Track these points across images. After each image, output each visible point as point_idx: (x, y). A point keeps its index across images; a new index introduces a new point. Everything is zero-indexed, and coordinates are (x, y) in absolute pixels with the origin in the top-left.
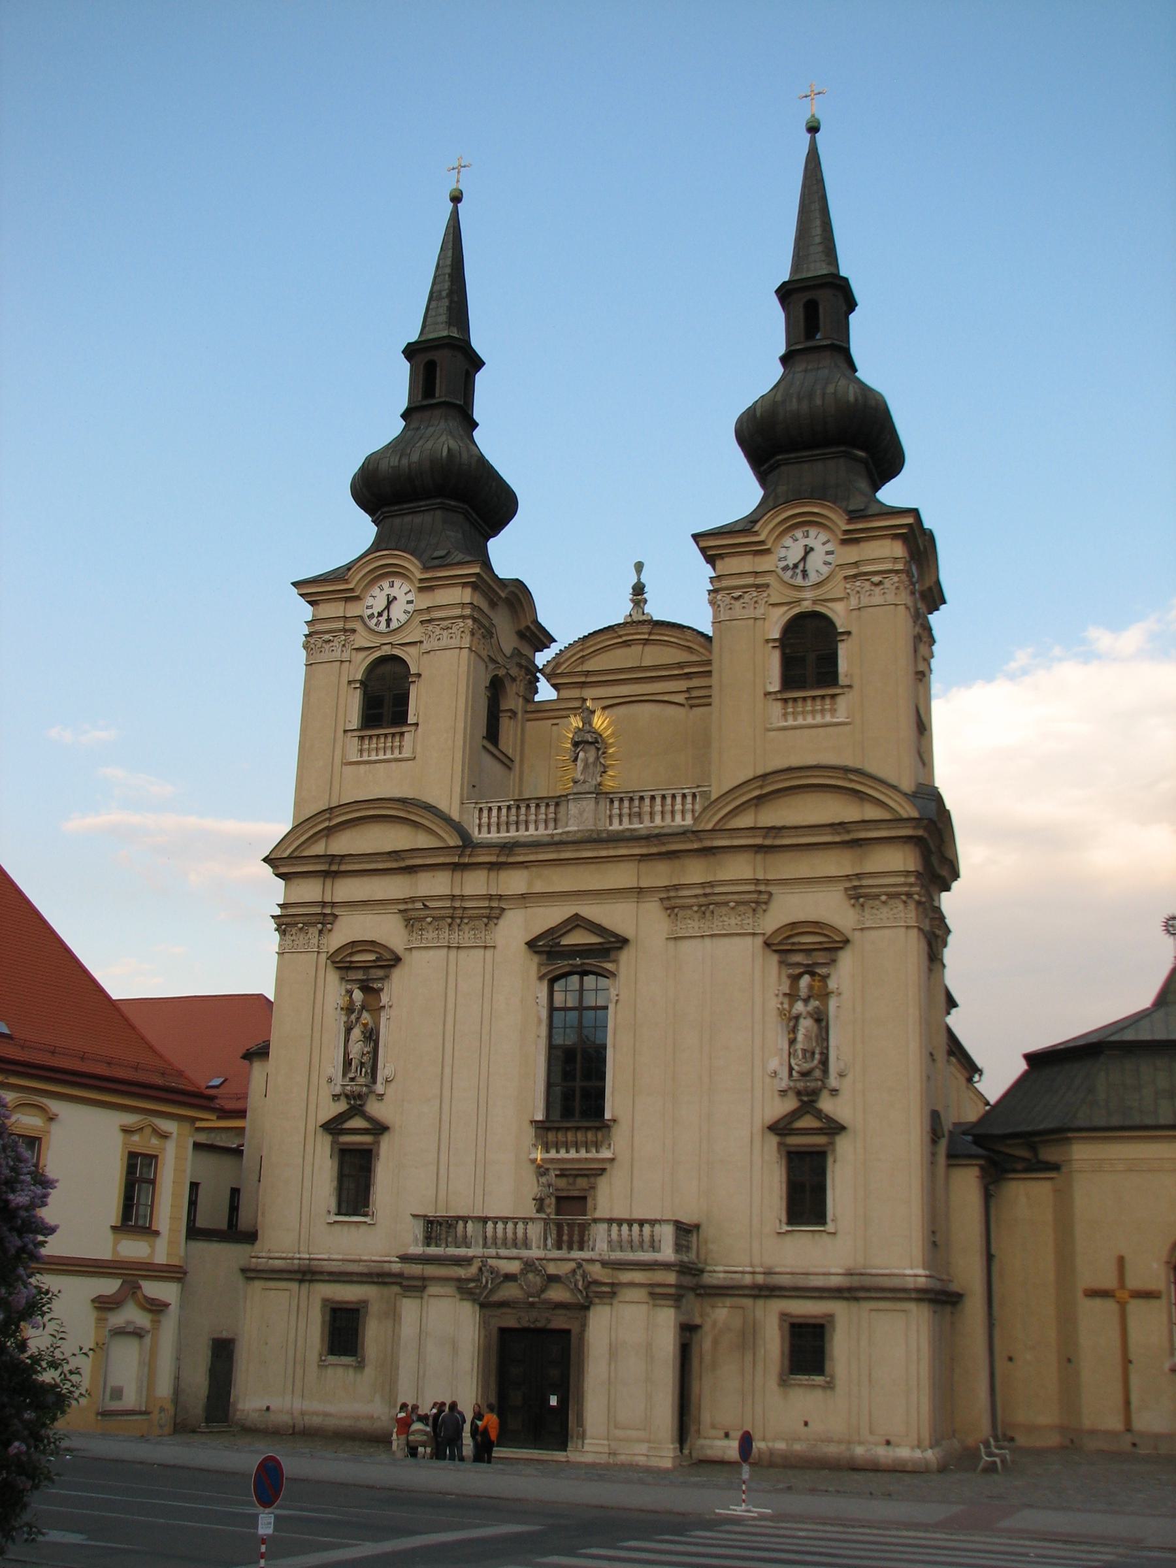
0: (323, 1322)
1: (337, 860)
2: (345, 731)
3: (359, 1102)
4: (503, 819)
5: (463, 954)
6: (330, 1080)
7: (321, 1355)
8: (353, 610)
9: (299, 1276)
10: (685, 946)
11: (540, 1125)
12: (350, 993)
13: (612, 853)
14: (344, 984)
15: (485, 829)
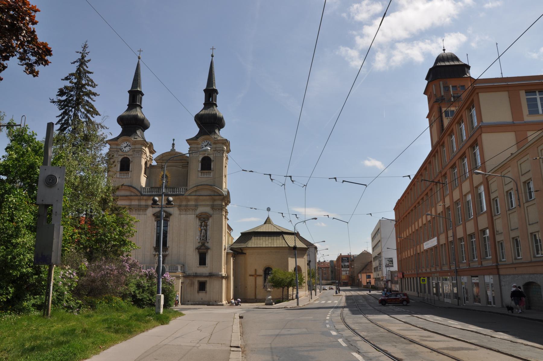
4: (148, 191)
5: (140, 216)
8: (119, 147)
10: (182, 216)
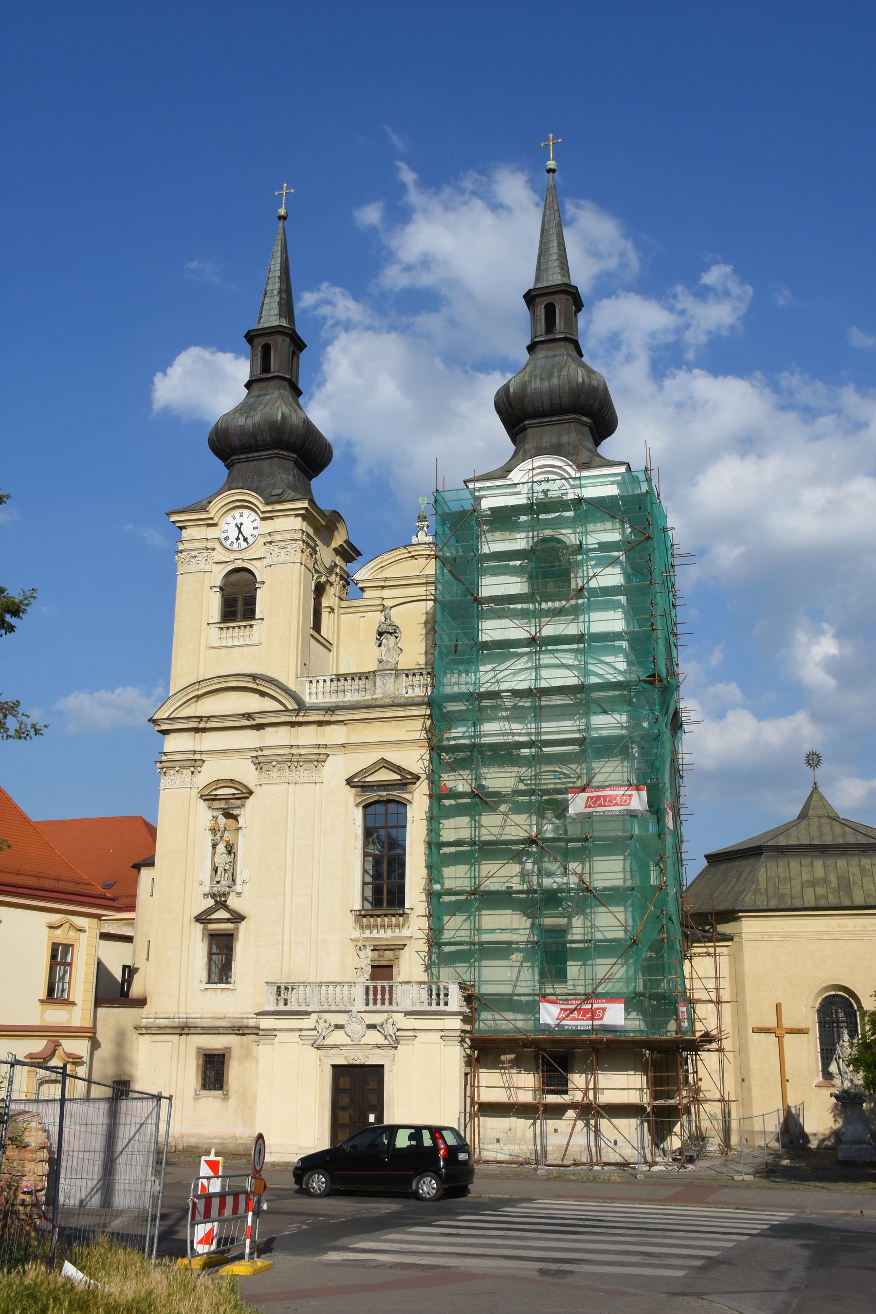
0: (198, 1065)
1: (204, 720)
2: (208, 624)
3: (223, 899)
6: (201, 883)
7: (196, 1091)
9: (179, 1031)
11: (358, 913)
12: (215, 818)
13: (408, 713)
14: (211, 811)
15: (314, 696)
